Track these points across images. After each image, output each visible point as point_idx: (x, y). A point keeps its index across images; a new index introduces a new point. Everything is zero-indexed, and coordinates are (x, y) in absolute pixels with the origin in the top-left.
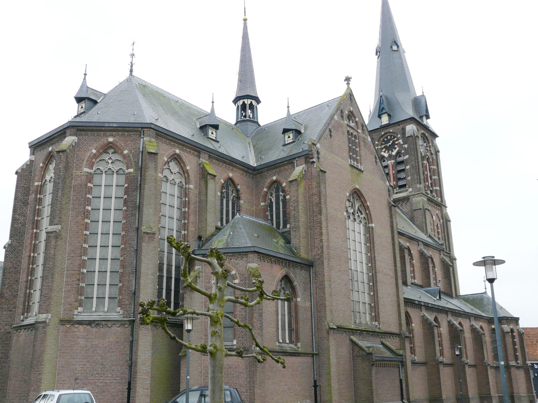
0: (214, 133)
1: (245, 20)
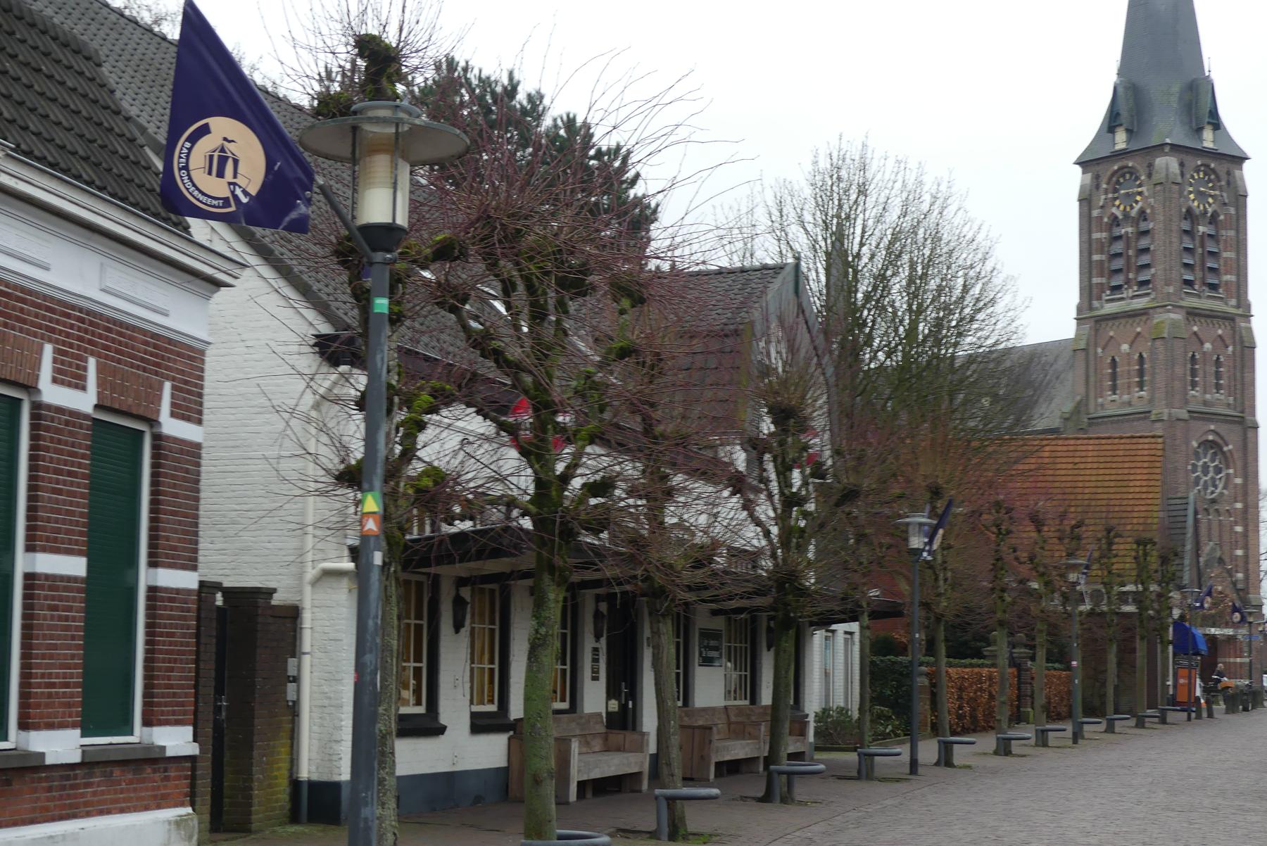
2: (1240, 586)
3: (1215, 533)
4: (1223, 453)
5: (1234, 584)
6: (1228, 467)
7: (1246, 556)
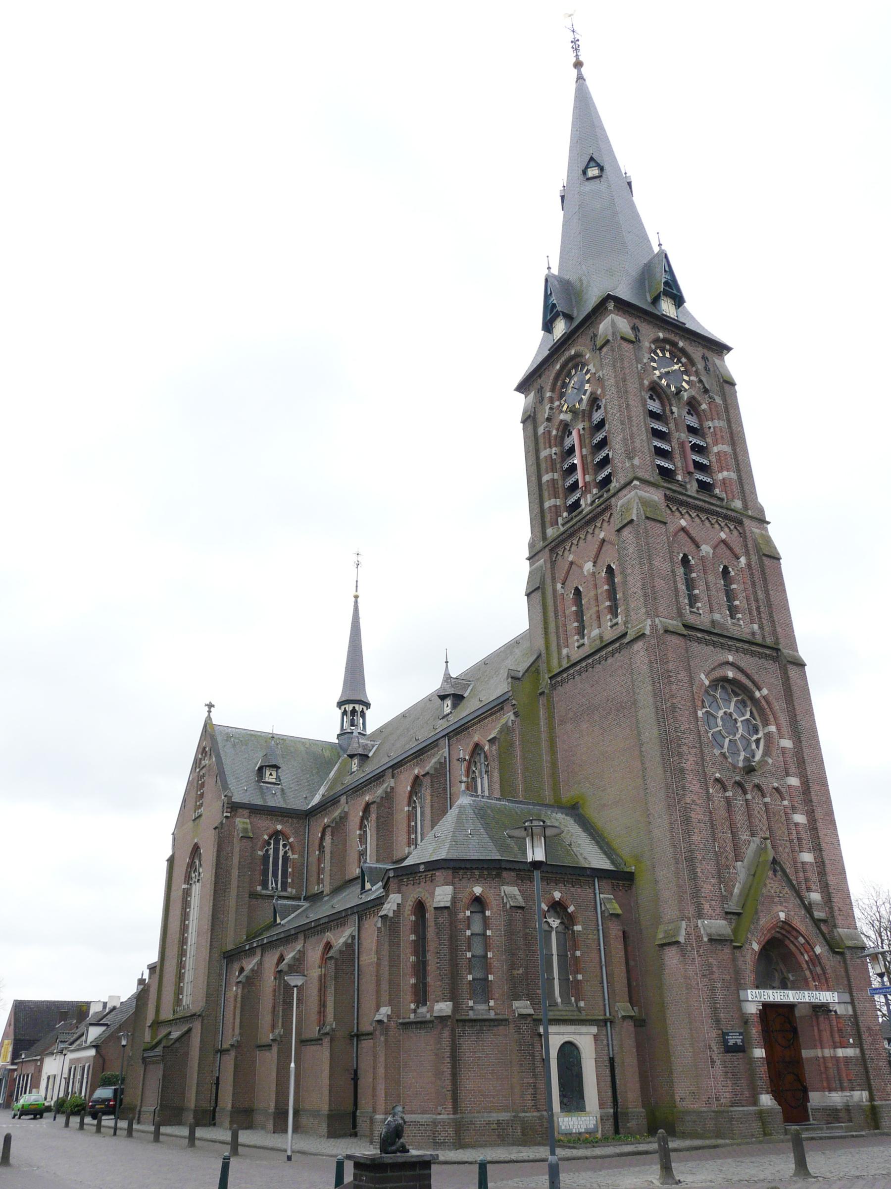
0: (274, 773)
1: (356, 597)
2: (819, 914)
3: (762, 825)
4: (755, 701)
5: (808, 908)
6: (766, 723)
7: (821, 864)
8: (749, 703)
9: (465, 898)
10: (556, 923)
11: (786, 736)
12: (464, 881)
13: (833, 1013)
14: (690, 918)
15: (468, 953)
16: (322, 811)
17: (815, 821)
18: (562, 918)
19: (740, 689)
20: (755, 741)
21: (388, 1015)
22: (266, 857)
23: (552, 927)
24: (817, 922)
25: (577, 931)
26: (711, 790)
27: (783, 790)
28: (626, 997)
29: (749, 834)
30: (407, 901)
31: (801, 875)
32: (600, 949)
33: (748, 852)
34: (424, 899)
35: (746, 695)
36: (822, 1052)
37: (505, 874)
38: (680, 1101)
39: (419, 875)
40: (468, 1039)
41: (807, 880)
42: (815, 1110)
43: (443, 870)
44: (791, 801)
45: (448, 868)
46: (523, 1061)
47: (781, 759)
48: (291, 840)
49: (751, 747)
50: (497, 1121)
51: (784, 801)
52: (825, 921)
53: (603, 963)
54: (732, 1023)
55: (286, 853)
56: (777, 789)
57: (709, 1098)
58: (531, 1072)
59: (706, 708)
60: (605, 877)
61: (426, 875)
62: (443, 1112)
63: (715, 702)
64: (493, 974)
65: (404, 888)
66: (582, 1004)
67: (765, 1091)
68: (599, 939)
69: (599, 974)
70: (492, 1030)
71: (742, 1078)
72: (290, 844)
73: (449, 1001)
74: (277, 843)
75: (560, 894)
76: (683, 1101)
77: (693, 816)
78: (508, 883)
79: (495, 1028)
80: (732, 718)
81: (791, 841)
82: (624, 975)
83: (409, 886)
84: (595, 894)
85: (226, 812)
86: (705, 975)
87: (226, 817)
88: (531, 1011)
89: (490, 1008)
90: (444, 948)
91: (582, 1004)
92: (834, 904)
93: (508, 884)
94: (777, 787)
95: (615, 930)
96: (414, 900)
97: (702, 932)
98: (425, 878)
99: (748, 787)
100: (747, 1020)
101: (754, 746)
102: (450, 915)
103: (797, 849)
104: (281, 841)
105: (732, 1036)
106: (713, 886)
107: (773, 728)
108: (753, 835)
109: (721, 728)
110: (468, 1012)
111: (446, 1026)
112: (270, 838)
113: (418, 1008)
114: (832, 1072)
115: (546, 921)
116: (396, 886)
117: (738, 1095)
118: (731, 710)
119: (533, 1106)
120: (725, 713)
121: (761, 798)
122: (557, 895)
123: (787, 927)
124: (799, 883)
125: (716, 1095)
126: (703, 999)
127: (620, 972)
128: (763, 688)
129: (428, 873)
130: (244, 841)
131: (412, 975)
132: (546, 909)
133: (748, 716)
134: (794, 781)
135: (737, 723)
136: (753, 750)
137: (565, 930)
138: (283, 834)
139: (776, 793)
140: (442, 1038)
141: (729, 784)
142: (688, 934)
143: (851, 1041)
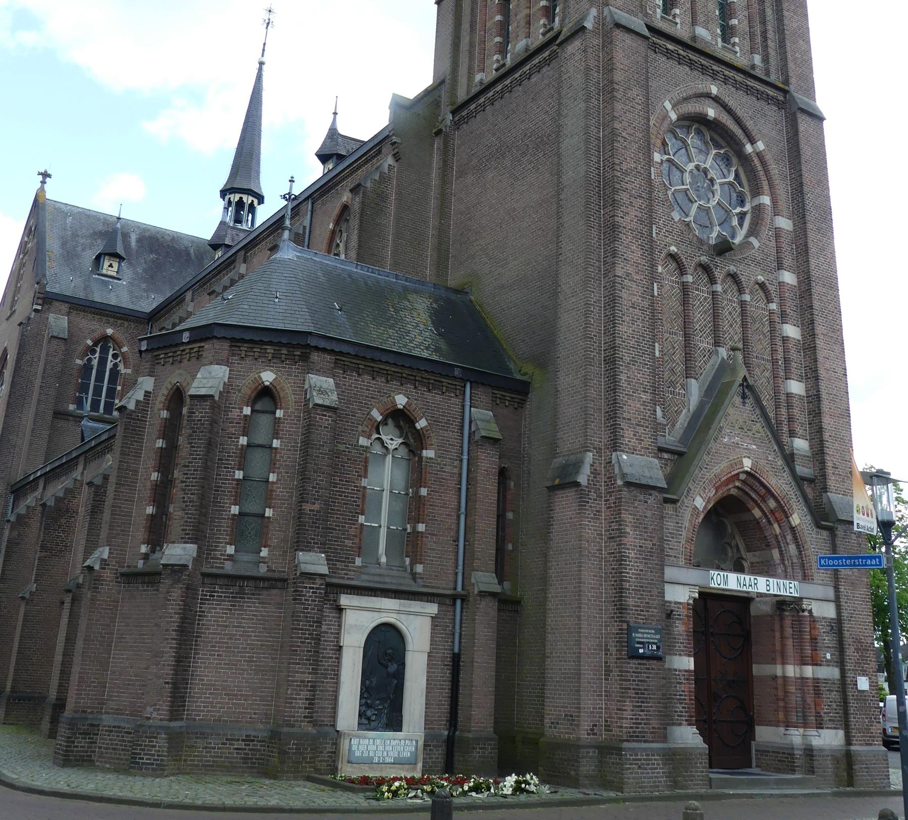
2: (802, 470)
3: (732, 331)
4: (744, 159)
5: (789, 459)
6: (756, 192)
7: (814, 398)
8: (734, 160)
9: (246, 387)
10: (395, 443)
11: (785, 213)
12: (248, 361)
13: (806, 614)
14: (600, 449)
15: (237, 472)
16: (165, 314)
17: (813, 335)
18: (406, 437)
19: (723, 138)
20: (737, 214)
21: (103, 560)
22: (88, 367)
23: (387, 448)
24: (799, 481)
25: (427, 458)
26: (660, 269)
27: (771, 288)
28: (492, 564)
29: (712, 341)
30: (160, 389)
31: (783, 411)
32: (460, 489)
33: (708, 367)
34: (184, 385)
35: (731, 147)
36: (784, 671)
37: (315, 357)
38: (550, 727)
39: (182, 348)
40: (216, 604)
41: (791, 419)
42: (762, 752)
43: (215, 341)
44: (781, 305)
45: (224, 338)
46: (299, 646)
47: (773, 244)
48: (125, 349)
49: (731, 222)
50: (246, 736)
51: (771, 304)
52: (811, 481)
53: (463, 510)
54: (646, 613)
55: (116, 365)
56: (762, 286)
57: (596, 725)
58: (310, 664)
59: (669, 155)
60: (483, 384)
61: (191, 349)
62: (153, 716)
63: (684, 150)
64: (274, 508)
65: (159, 368)
66: (419, 568)
67: (686, 720)
68: (460, 474)
69: (454, 526)
70: (259, 594)
71: (650, 698)
72: (122, 353)
73: (191, 543)
74: (105, 351)
75: (407, 399)
76: (555, 728)
77: (625, 296)
78: (317, 370)
79: (265, 592)
80: (706, 176)
81: (774, 362)
82: (492, 530)
83: (166, 366)
84: (463, 406)
85: (36, 304)
86: (613, 538)
87: (36, 311)
88: (324, 570)
89: (263, 561)
90: (195, 459)
91: (419, 568)
92: (827, 457)
93: (318, 372)
94: (763, 282)
95: (488, 461)
96: (170, 387)
97: (617, 471)
98: (190, 353)
99: (719, 275)
100: (672, 611)
101: (735, 222)
102: (212, 408)
103: (782, 374)
104: (111, 349)
105: (643, 633)
106: (644, 404)
107: (766, 200)
108: (717, 344)
109: (688, 187)
110: (223, 563)
111: (179, 581)
112: (96, 344)
113: (154, 552)
114: (795, 698)
115: (379, 439)
116: (148, 365)
117: (641, 724)
118: (708, 165)
119: (305, 717)
120: (697, 167)
121: (736, 294)
122: (401, 401)
123: (751, 481)
124: (779, 423)
125: (606, 721)
126: (606, 573)
127: (486, 525)
128: (759, 140)
129: (194, 346)
130: (55, 342)
131: (150, 501)
132: (379, 418)
133: (731, 178)
134: (789, 278)
135: (713, 185)
136: (733, 228)
137: (410, 456)
138: (114, 341)
139: (760, 291)
140: (170, 600)
141: (690, 265)
142: (595, 473)
143: (828, 656)
